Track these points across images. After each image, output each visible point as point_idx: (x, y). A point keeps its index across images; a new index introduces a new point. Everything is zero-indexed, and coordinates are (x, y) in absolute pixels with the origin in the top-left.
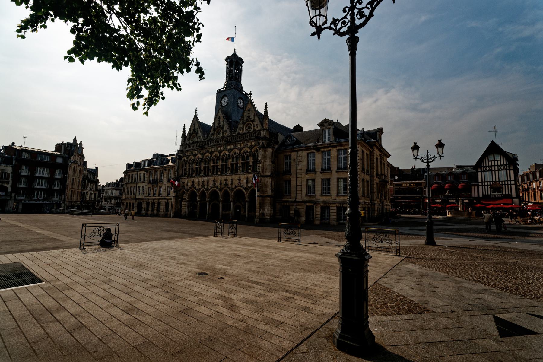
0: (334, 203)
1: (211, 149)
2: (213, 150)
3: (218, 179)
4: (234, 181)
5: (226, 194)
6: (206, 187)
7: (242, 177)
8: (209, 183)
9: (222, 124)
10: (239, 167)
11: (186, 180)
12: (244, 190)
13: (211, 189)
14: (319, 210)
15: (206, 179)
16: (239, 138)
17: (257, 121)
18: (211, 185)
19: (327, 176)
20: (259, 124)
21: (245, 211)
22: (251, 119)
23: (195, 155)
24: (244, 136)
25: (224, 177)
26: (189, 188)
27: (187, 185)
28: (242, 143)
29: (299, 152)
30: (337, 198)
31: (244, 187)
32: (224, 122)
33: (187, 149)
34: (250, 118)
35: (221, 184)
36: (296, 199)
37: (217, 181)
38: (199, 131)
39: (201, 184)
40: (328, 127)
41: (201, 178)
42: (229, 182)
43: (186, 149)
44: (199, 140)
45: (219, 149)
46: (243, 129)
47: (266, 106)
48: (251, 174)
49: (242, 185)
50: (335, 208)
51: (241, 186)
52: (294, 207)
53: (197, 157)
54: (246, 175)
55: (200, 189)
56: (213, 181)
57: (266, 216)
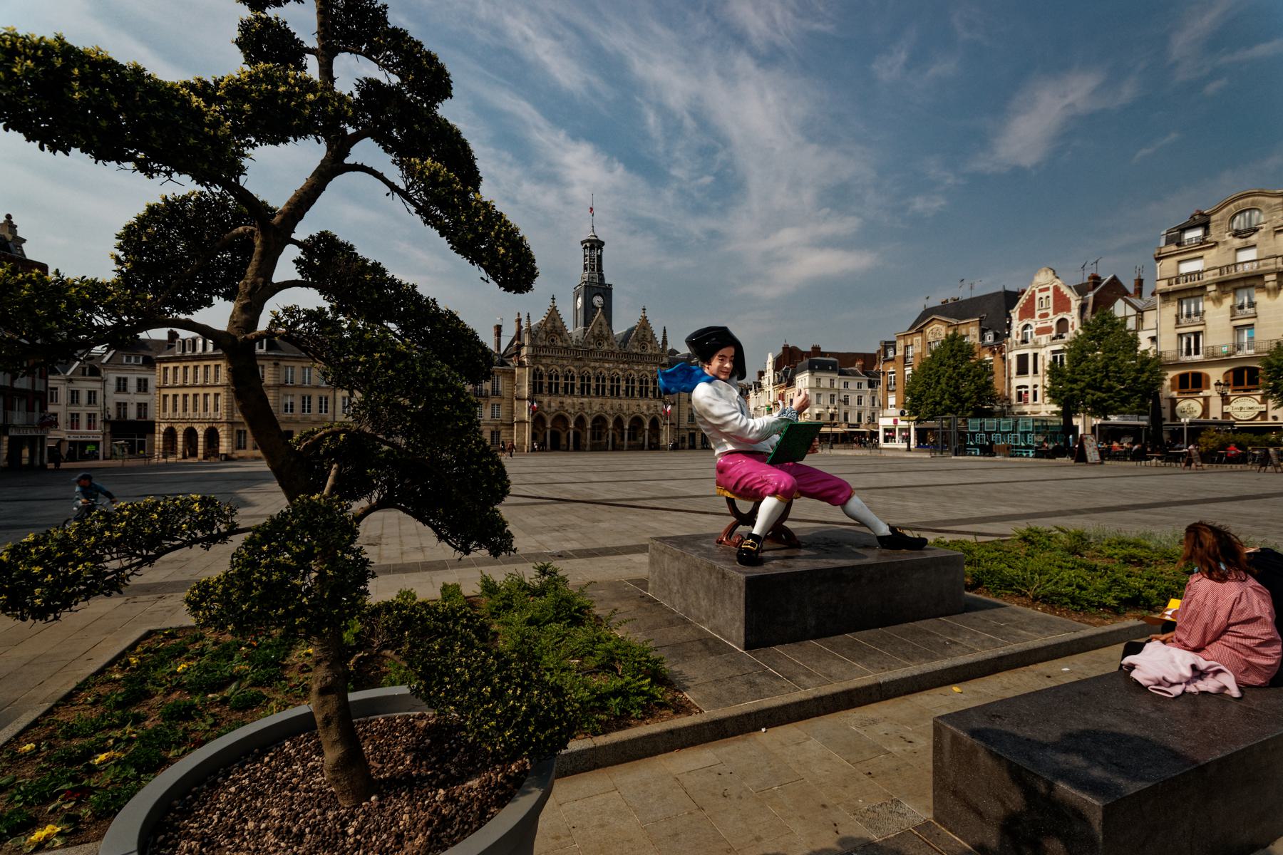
2: (597, 364)
5: (580, 421)
7: (641, 403)
11: (546, 400)
15: (585, 400)
21: (623, 439)
23: (562, 366)
26: (553, 410)
27: (549, 406)
39: (577, 408)
44: (565, 345)
45: (607, 365)
53: (566, 369)
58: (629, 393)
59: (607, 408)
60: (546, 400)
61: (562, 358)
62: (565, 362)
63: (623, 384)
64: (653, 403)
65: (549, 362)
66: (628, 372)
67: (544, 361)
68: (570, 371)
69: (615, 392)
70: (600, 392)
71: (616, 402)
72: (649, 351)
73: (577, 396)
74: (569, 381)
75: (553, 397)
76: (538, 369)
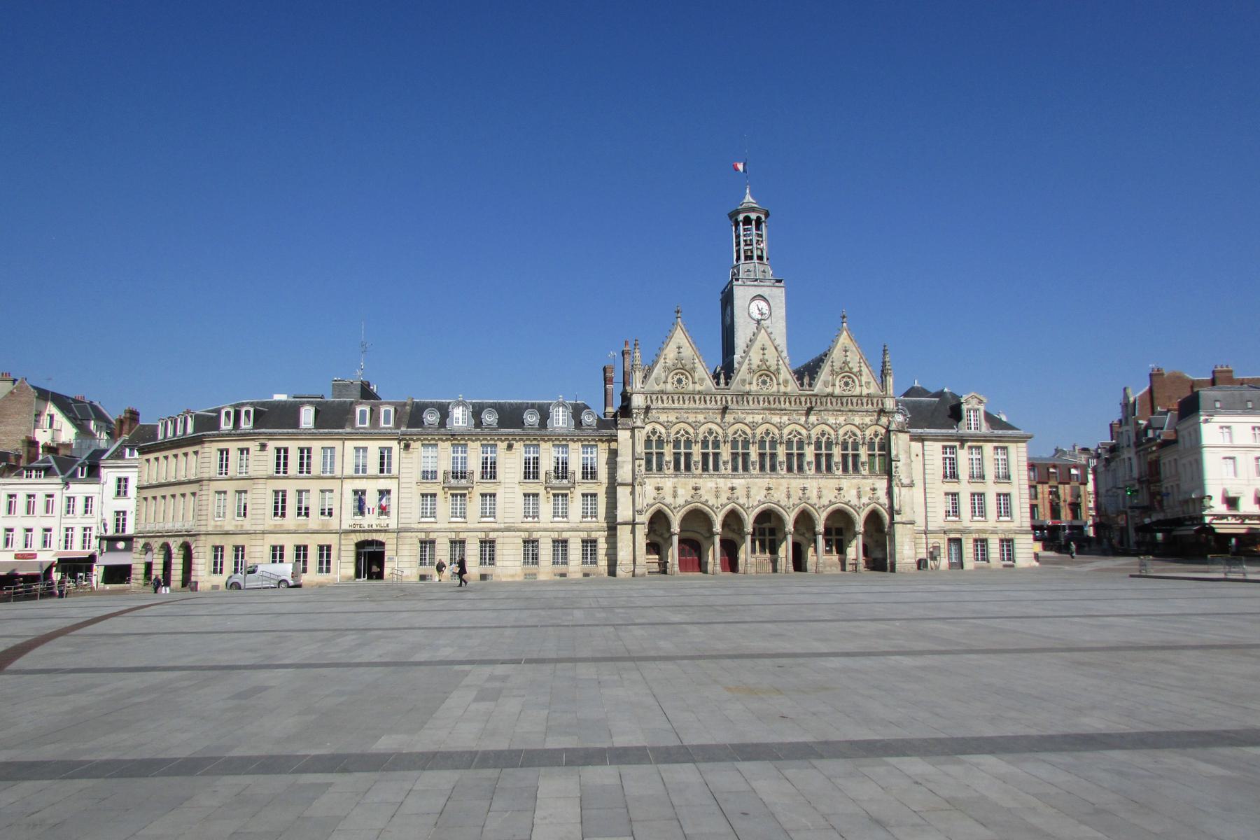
0: (994, 532)
1: (751, 416)
2: (758, 418)
3: (780, 485)
4: (824, 492)
6: (741, 501)
8: (752, 493)
9: (772, 363)
10: (863, 464)
12: (852, 510)
13: (758, 506)
14: (971, 546)
15: (737, 482)
16: (831, 403)
17: (867, 375)
18: (758, 498)
19: (978, 488)
20: (871, 384)
22: (851, 369)
24: (845, 400)
25: (797, 480)
26: (680, 501)
28: (842, 415)
29: (926, 443)
30: (998, 525)
31: (852, 503)
32: (778, 361)
33: (665, 405)
34: (850, 365)
35: (789, 497)
36: (926, 527)
37: (776, 489)
38: (698, 365)
40: (976, 407)
41: (722, 480)
42: (811, 492)
43: (660, 405)
45: (776, 419)
46: (834, 385)
47: (884, 351)
48: (868, 478)
49: (846, 500)
50: (998, 541)
51: (846, 504)
52: (924, 541)
54: (854, 481)
55: (724, 506)
56: (769, 489)
57: (908, 558)
58: (824, 465)
59: (779, 496)
60: (668, 484)
61: (697, 411)
62: (701, 418)
63: (810, 452)
64: (867, 484)
65: (672, 418)
66: (819, 429)
67: (663, 418)
68: (711, 432)
69: (795, 464)
70: (768, 464)
71: (796, 483)
72: (857, 391)
73: (724, 476)
74: (711, 450)
75: (681, 480)
76: (654, 432)
